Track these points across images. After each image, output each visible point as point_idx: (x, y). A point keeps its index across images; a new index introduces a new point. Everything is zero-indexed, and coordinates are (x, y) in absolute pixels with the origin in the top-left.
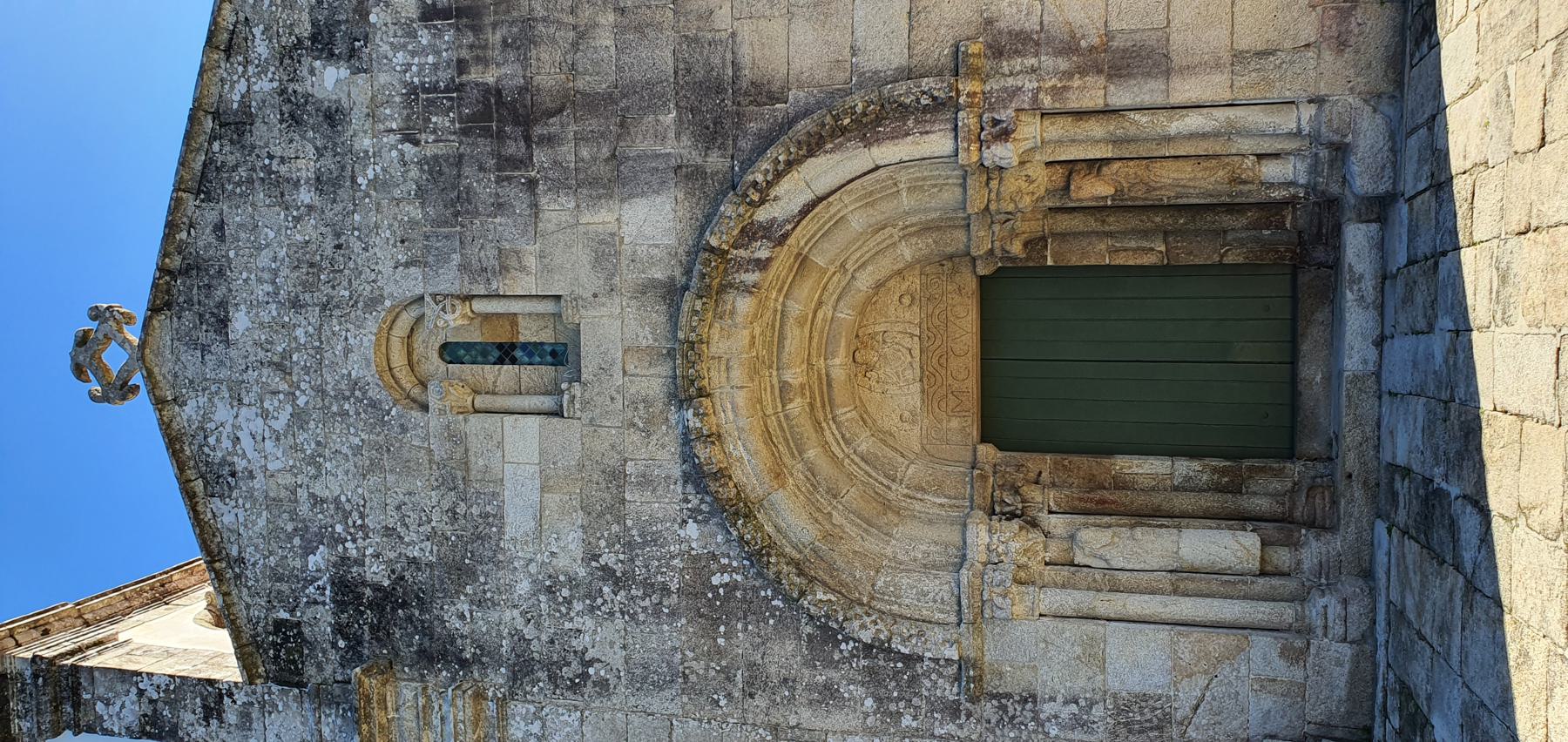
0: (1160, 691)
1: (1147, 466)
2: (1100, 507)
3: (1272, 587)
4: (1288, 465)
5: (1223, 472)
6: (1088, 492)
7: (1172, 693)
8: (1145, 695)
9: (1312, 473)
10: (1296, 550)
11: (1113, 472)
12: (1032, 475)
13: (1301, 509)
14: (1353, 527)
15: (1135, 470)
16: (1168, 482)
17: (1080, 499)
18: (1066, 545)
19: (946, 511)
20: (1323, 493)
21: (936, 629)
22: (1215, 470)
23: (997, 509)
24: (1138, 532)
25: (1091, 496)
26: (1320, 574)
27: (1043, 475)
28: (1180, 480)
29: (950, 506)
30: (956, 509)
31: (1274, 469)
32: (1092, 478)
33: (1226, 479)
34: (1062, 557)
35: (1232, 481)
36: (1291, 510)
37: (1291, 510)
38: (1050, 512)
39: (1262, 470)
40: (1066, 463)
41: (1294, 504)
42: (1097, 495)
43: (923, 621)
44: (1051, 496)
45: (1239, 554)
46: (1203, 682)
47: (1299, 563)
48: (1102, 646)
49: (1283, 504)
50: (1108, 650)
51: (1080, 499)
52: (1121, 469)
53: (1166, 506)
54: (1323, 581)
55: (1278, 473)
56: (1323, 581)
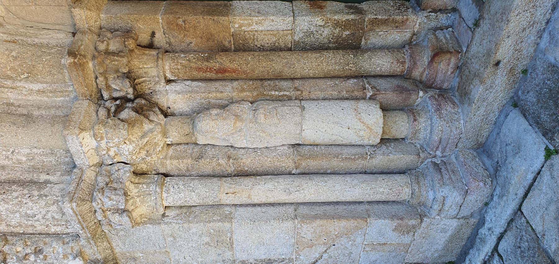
0: (283, 257)
1: (267, 22)
2: (220, 75)
3: (392, 161)
4: (412, 17)
5: (346, 25)
6: (207, 59)
7: (294, 257)
8: (270, 260)
9: (433, 24)
10: (415, 120)
11: (232, 30)
12: (144, 38)
13: (421, 70)
14: (482, 110)
15: (255, 27)
16: (289, 37)
17: (199, 69)
18: (187, 129)
19: (48, 97)
20: (449, 59)
21: (54, 244)
22: (337, 24)
23: (106, 95)
24: (264, 108)
25: (209, 65)
26: (438, 148)
27: (157, 35)
28: (301, 35)
29: (51, 92)
30: (59, 93)
31: (396, 22)
32: (210, 37)
33: (347, 33)
34: (184, 140)
35: (353, 35)
36: (410, 70)
37: (410, 70)
38: (169, 81)
39: (385, 22)
40: (180, 22)
41: (415, 63)
42: (215, 64)
43: (39, 234)
44: (167, 67)
45: (362, 133)
46: (322, 249)
47: (415, 133)
48: (229, 235)
49: (403, 63)
50: (235, 237)
51: (199, 69)
52: (241, 26)
53: (287, 72)
54: (439, 153)
55: (399, 25)
56: (439, 153)
